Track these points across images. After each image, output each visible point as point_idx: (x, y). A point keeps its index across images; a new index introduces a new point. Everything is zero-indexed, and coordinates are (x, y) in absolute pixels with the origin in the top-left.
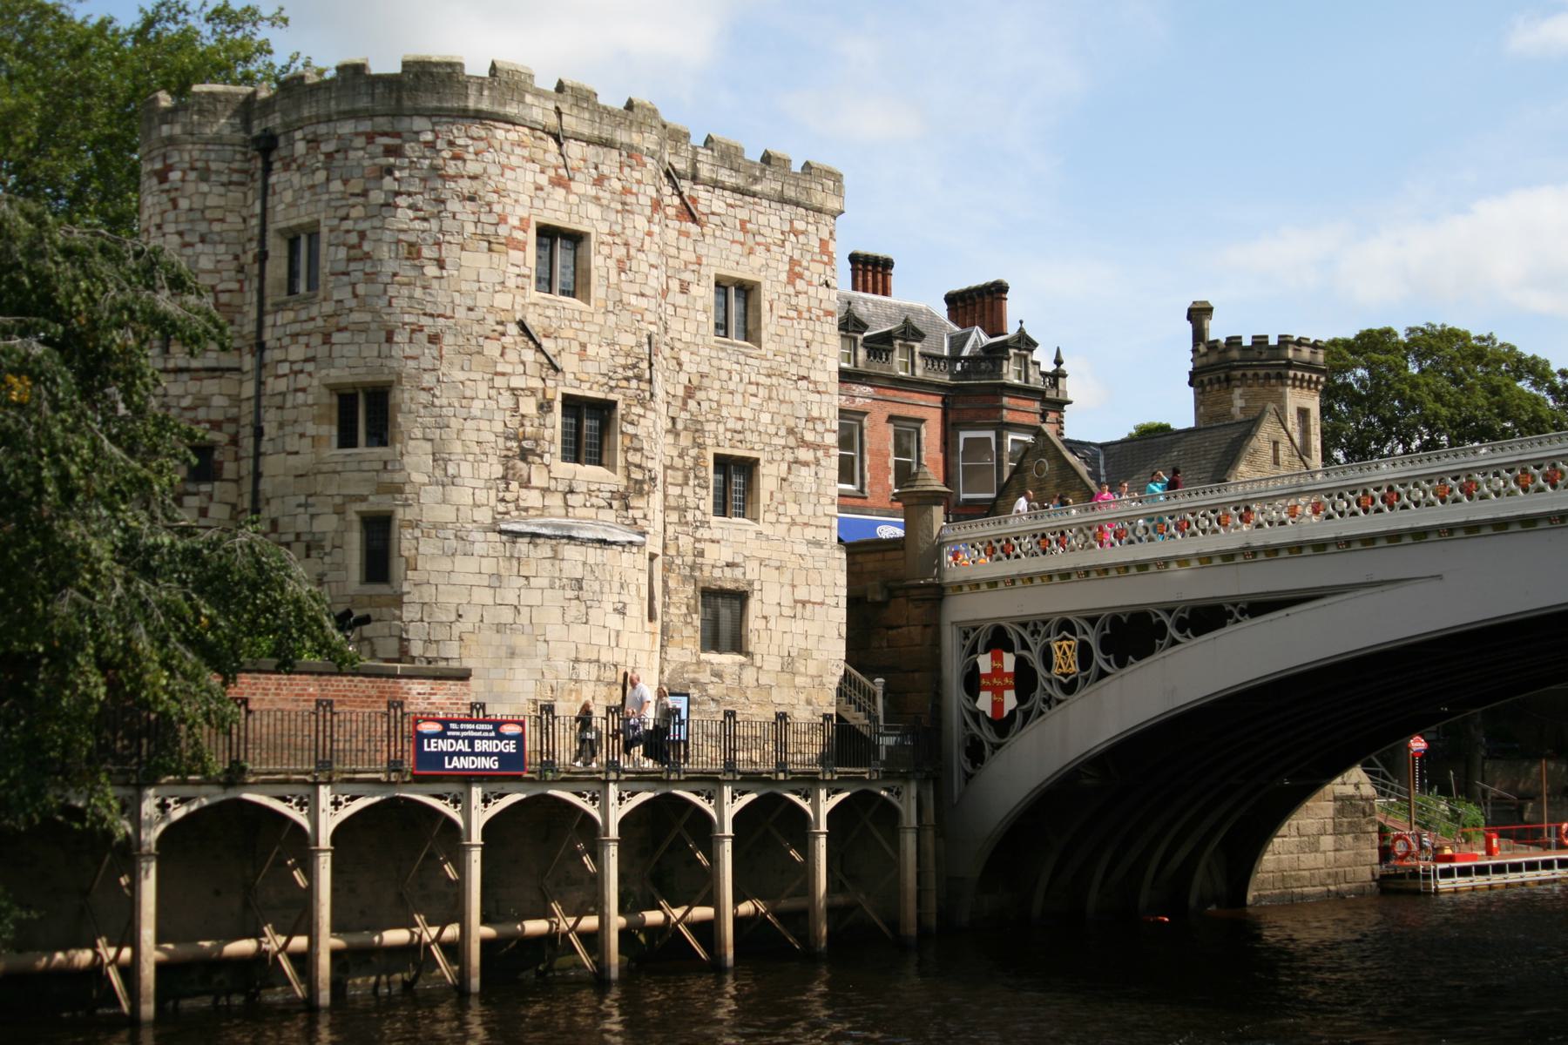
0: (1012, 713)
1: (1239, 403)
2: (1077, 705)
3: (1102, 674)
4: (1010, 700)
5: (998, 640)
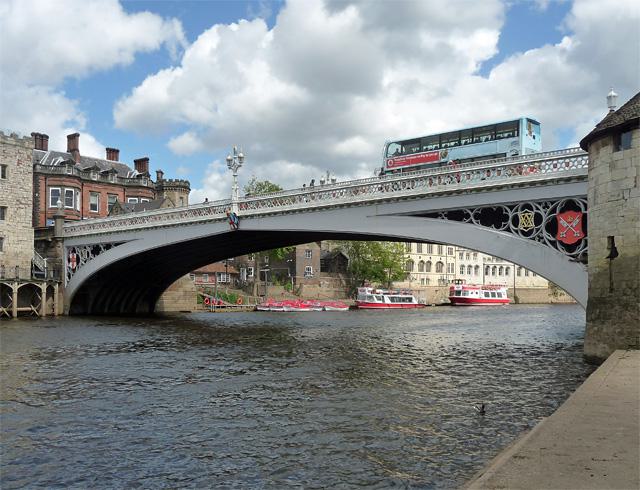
2: (86, 265)
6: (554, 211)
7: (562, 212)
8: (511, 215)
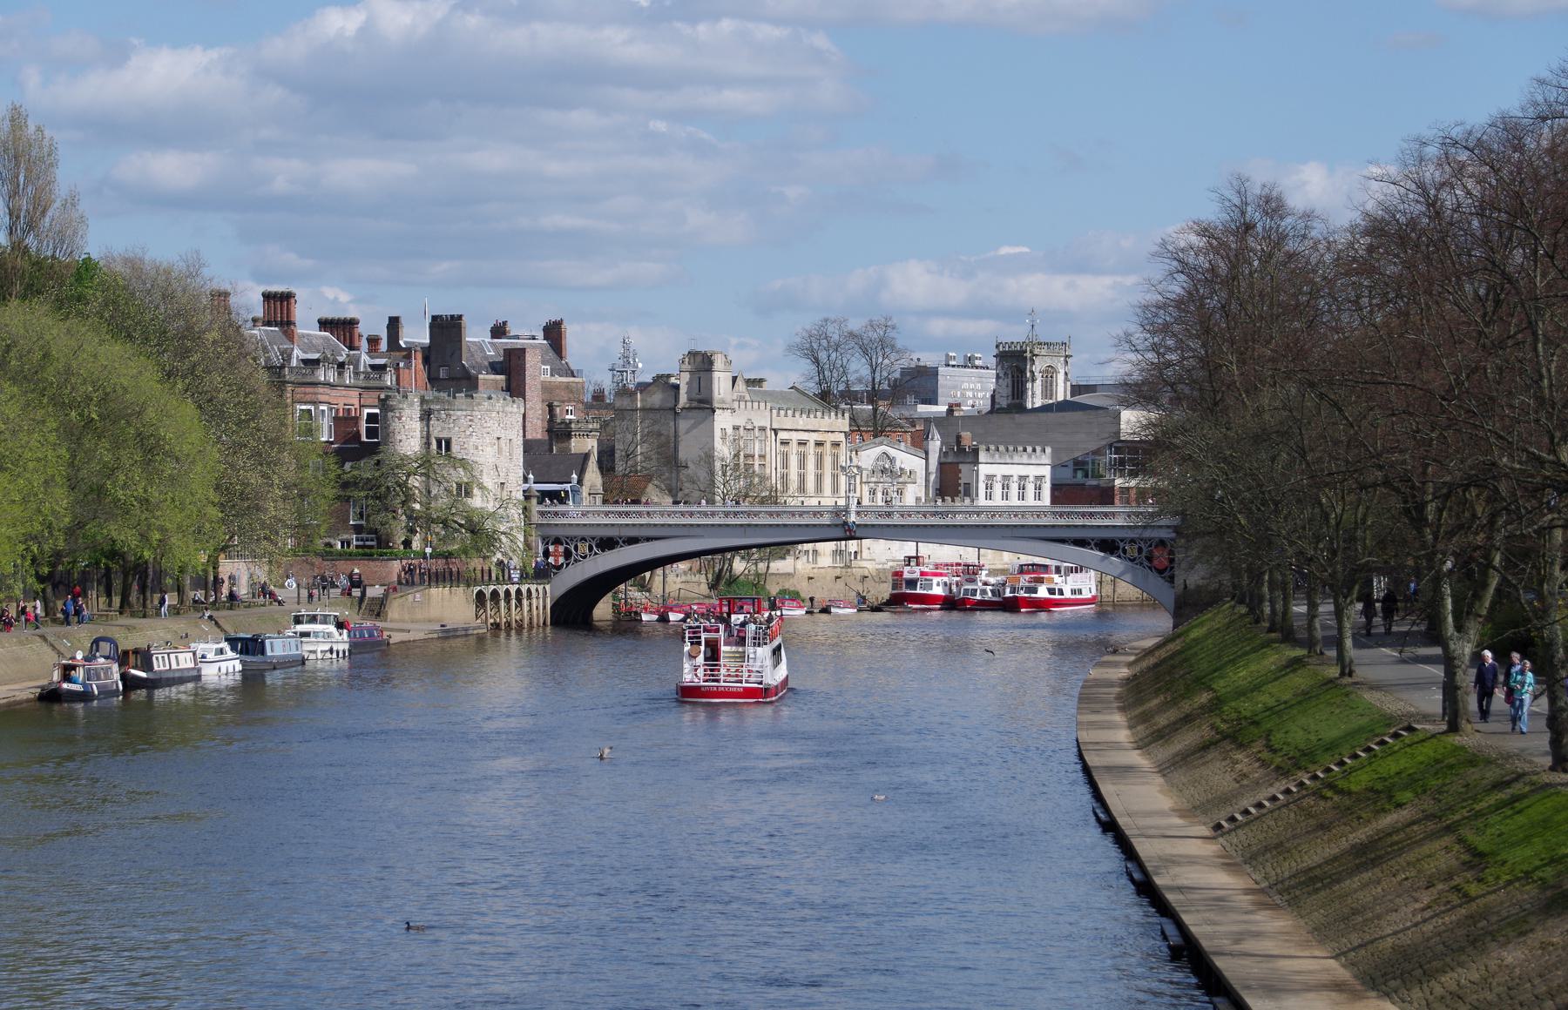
0: (562, 564)
1: (573, 444)
3: (596, 554)
4: (561, 560)
5: (557, 541)
6: (1150, 546)
7: (1156, 547)
8: (1121, 545)
